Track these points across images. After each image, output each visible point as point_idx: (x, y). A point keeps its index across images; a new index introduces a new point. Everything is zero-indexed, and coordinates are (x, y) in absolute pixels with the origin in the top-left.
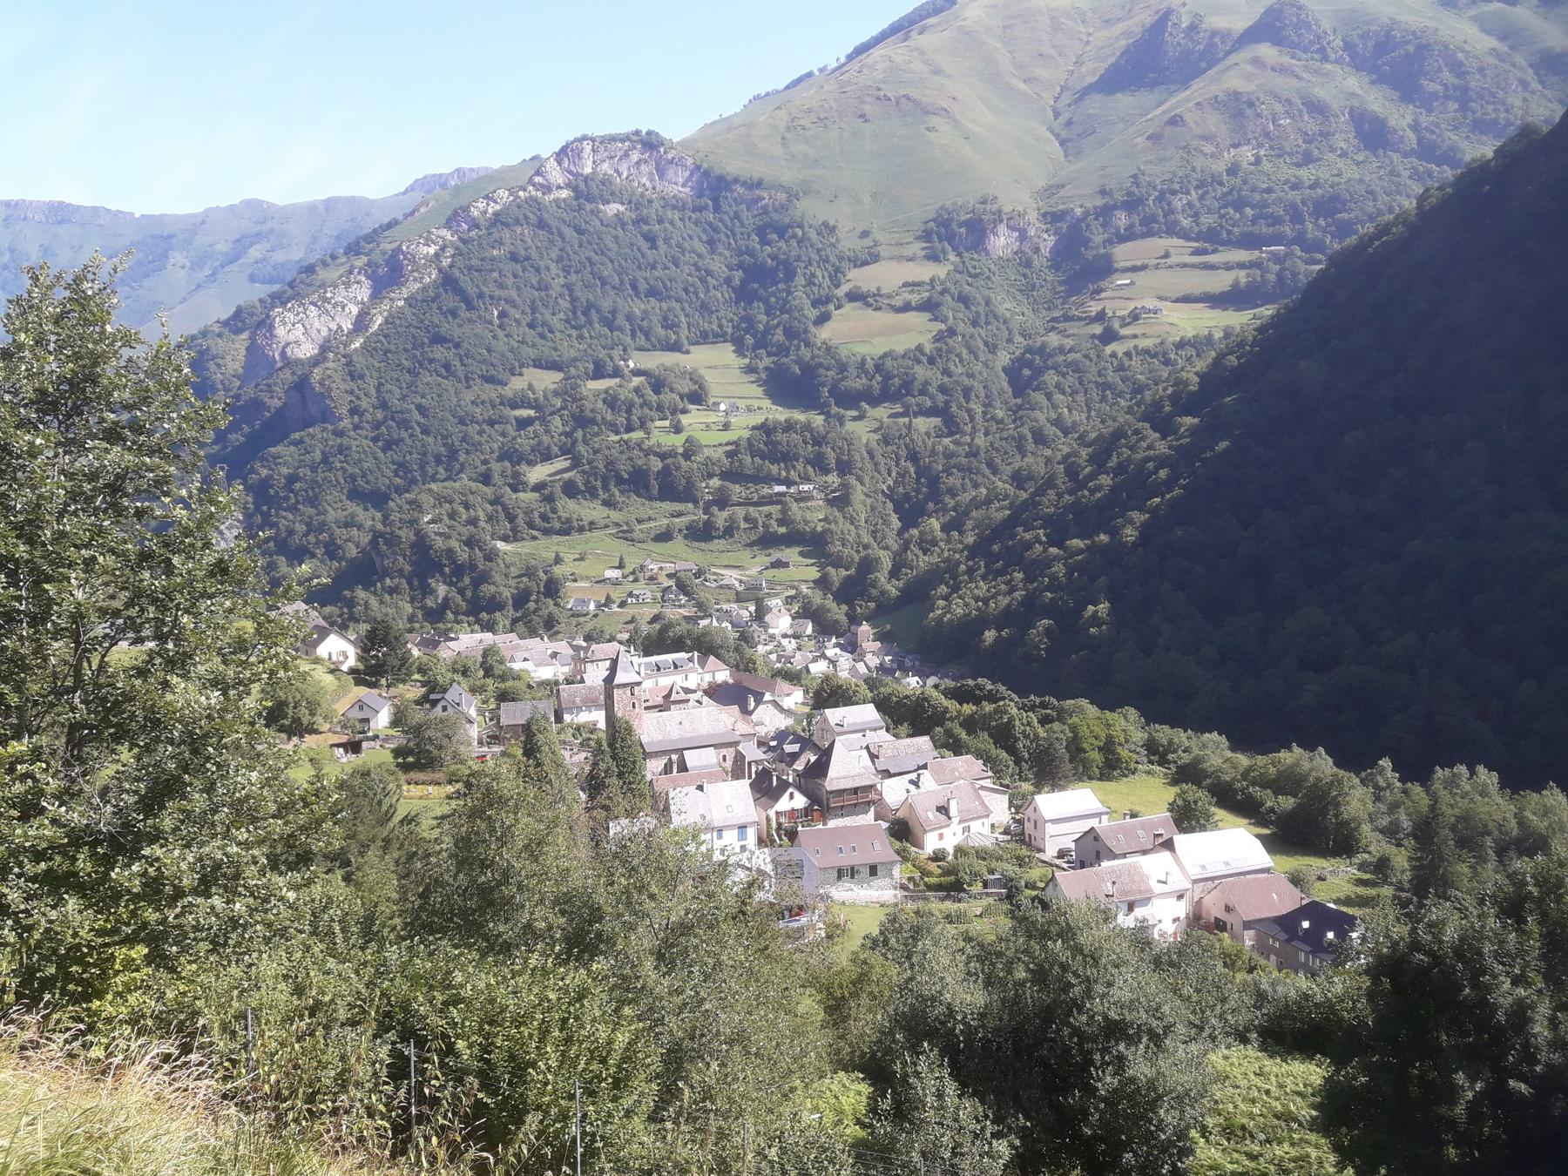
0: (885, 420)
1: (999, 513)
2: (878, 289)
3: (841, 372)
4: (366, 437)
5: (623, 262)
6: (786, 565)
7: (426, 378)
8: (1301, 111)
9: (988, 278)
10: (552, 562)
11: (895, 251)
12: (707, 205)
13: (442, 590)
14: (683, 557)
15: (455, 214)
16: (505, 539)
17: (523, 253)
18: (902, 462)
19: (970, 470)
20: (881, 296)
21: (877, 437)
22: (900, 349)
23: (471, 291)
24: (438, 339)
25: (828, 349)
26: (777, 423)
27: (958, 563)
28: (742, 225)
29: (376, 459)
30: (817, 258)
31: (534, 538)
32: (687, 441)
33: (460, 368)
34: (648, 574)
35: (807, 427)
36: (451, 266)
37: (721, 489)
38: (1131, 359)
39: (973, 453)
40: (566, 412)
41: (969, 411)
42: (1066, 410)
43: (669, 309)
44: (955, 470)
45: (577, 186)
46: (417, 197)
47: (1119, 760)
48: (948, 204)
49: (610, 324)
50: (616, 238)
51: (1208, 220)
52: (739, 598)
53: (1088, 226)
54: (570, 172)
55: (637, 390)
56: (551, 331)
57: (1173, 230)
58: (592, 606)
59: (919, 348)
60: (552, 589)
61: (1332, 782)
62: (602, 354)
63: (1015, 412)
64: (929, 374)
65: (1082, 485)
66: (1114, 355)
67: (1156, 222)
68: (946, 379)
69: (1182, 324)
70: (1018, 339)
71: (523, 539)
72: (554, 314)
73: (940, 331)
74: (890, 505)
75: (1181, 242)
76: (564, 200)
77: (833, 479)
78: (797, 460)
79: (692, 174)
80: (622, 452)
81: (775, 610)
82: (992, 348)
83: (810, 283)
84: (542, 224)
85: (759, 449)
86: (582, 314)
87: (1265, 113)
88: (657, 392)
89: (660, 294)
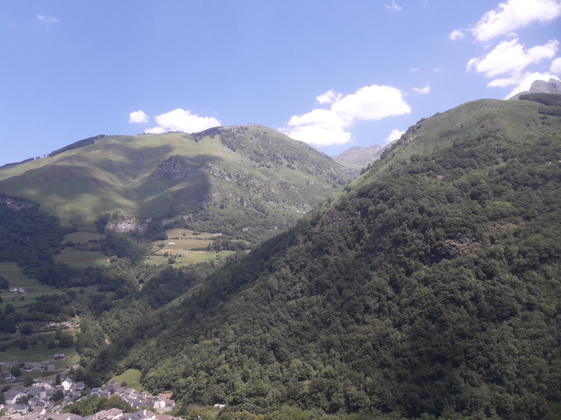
2: (79, 243)
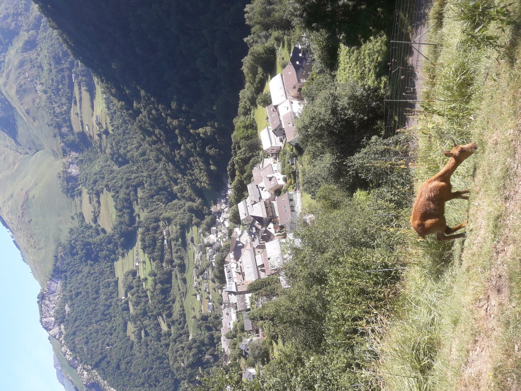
0: (139, 207)
1: (170, 167)
2: (92, 212)
3: (123, 223)
4: (155, 389)
5: (87, 303)
6: (192, 238)
7: (132, 370)
8: (23, 69)
9: (87, 174)
10: (195, 319)
11: (78, 207)
12: (64, 275)
13: (207, 357)
14: (191, 273)
15: (71, 366)
16: (188, 336)
17: (85, 340)
18: (154, 200)
19: (156, 177)
20: (95, 211)
21: (145, 210)
22: (114, 203)
23: (100, 357)
24: (118, 367)
25: (114, 228)
26: (142, 245)
27: (188, 179)
28: (71, 262)
29: (162, 385)
30: (82, 234)
31: (187, 326)
32: (150, 276)
33: (128, 359)
34: (198, 285)
35: (143, 234)
36: (91, 365)
37: (167, 262)
38: (114, 125)
39: (150, 176)
40: (142, 320)
41: (135, 179)
42: (133, 146)
43: (103, 286)
44: (156, 182)
45: (59, 322)
46: (65, 381)
47: (250, 124)
48: (61, 189)
49: (109, 306)
50: (78, 306)
51: (64, 100)
52: (205, 253)
53: (67, 141)
54: (54, 325)
55: (132, 295)
56: (113, 327)
57: (68, 112)
58: (210, 304)
59: (113, 197)
60: (205, 318)
61: (252, 55)
62: (120, 308)
63: (135, 163)
64: (122, 193)
65: (159, 139)
66: (113, 130)
67: (65, 118)
68: (124, 187)
69: (101, 108)
70: (108, 163)
71: (188, 330)
72: (107, 327)
73: (107, 190)
74: (169, 204)
75: (72, 109)
76: (64, 326)
77: (161, 224)
78: (155, 236)
79: (53, 281)
80: (155, 298)
81: (208, 240)
82: (112, 172)
83: (91, 236)
84: (74, 334)
85: (152, 250)
86: (106, 316)
87: (24, 81)
88: (133, 288)
89: (97, 290)
